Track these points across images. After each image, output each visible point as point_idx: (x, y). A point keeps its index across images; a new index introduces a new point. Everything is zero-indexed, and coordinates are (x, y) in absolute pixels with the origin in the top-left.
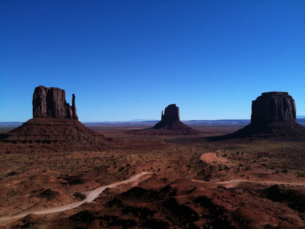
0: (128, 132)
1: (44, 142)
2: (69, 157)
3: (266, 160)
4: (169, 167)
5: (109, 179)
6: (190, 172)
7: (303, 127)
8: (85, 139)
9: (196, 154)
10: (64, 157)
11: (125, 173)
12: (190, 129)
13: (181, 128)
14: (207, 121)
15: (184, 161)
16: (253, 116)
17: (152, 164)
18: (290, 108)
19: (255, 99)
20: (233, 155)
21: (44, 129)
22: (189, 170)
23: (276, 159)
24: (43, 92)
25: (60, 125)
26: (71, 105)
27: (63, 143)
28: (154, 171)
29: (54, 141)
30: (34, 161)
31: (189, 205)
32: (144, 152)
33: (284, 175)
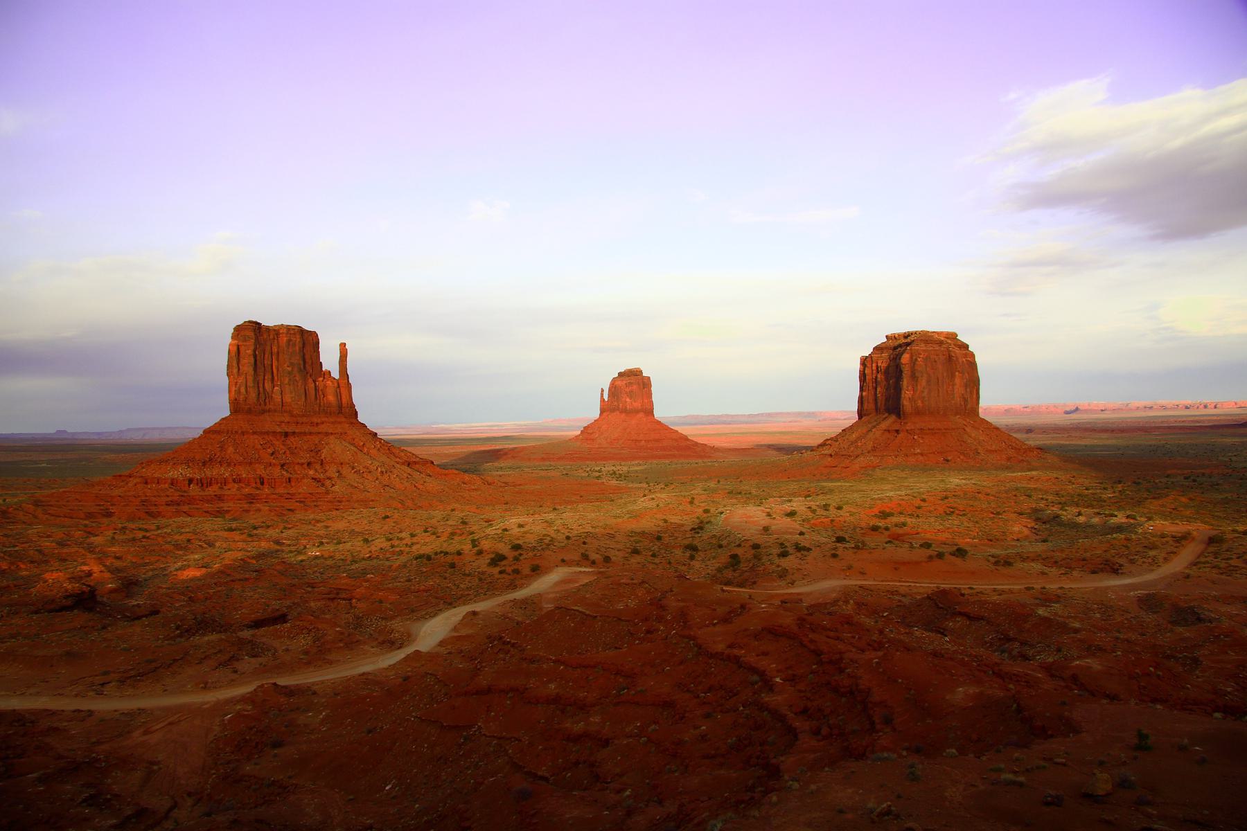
4: (636, 552)
5: (462, 586)
6: (693, 563)
7: (997, 429)
9: (706, 511)
10: (327, 527)
11: (509, 569)
12: (688, 440)
15: (676, 535)
17: (584, 543)
20: (814, 511)
22: (692, 558)
26: (336, 374)
28: (593, 562)
31: (736, 651)
32: (555, 509)
33: (958, 561)
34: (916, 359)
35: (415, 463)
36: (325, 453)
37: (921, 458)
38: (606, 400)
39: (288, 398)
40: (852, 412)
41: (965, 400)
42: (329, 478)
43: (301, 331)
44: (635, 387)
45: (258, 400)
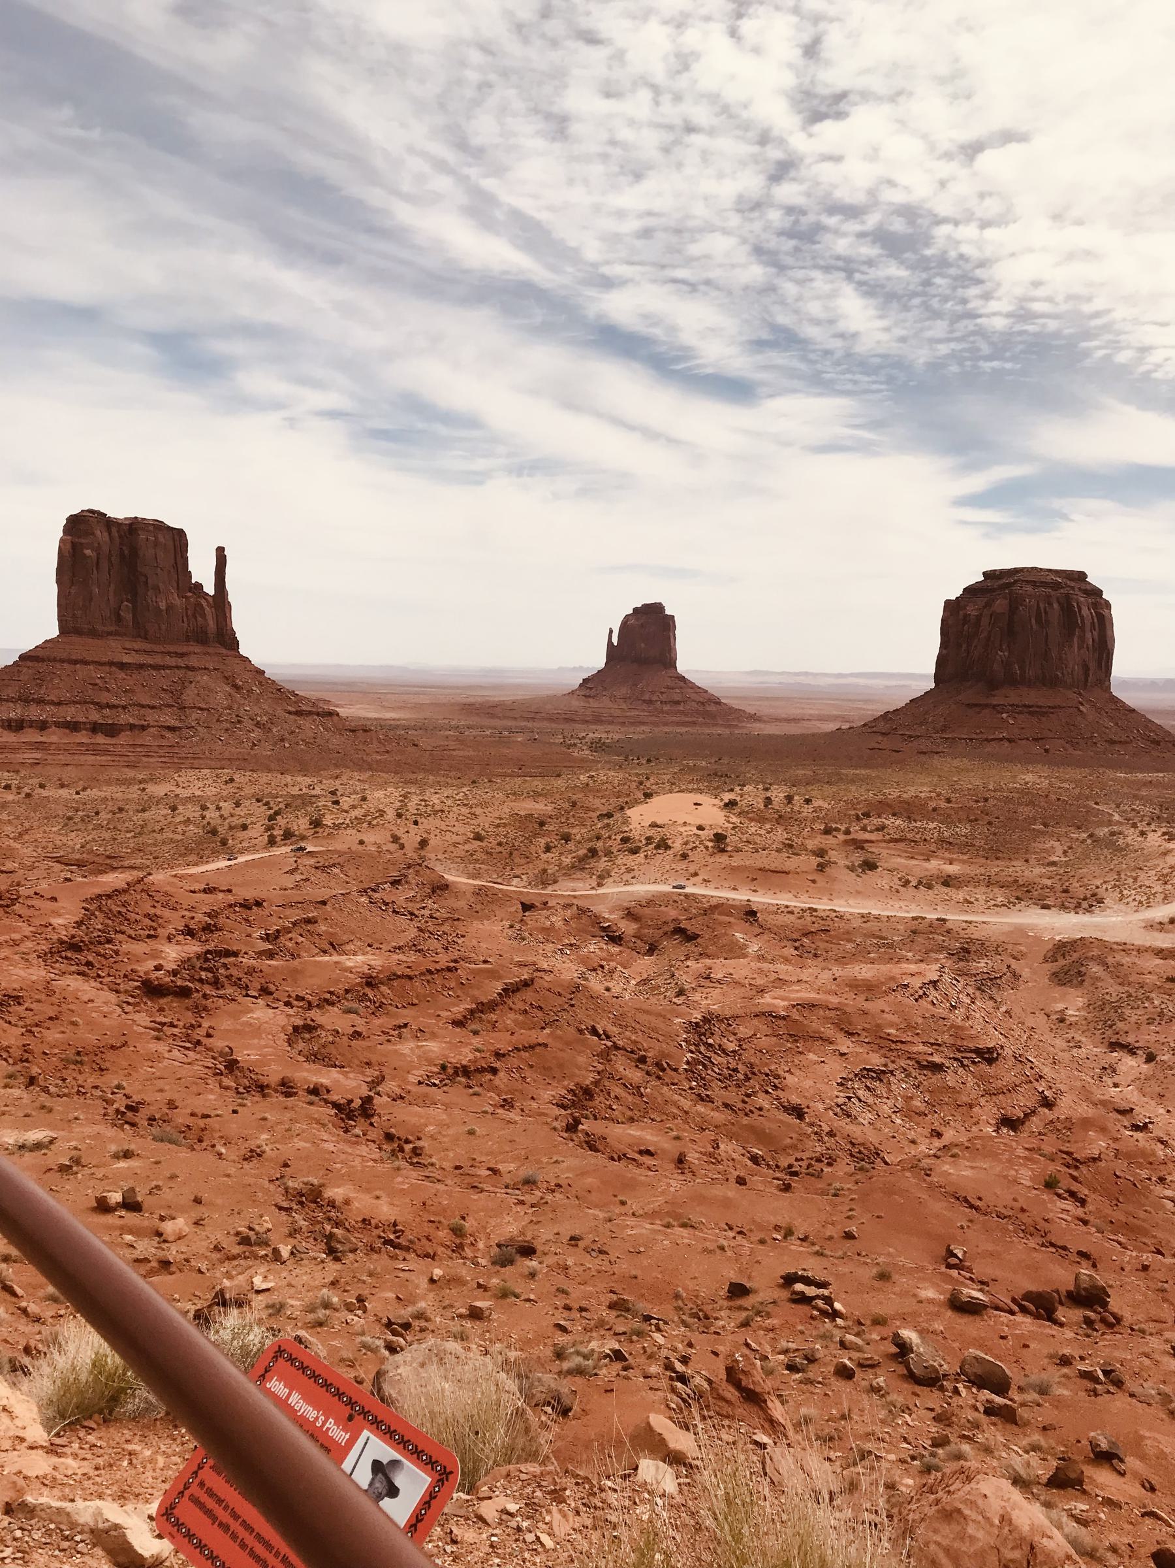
0: (469, 708)
1: (95, 728)
2: (159, 790)
3: (881, 828)
4: (478, 837)
8: (258, 724)
12: (717, 702)
13: (677, 698)
14: (812, 674)
16: (941, 662)
17: (416, 823)
18: (1088, 635)
19: (955, 593)
21: (98, 681)
23: (932, 825)
24: (98, 533)
25: (164, 667)
26: (210, 589)
27: (168, 735)
29: (132, 727)
30: (17, 798)
34: (1017, 608)
35: (310, 713)
36: (189, 697)
37: (1007, 744)
38: (615, 641)
40: (922, 677)
41: (1086, 669)
43: (159, 526)
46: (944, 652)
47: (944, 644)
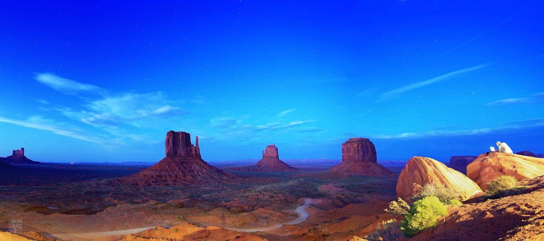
16: (343, 156)
26: (195, 146)
39: (182, 153)
42: (196, 175)
44: (273, 150)
45: (174, 153)
46: (344, 154)
47: (343, 152)
